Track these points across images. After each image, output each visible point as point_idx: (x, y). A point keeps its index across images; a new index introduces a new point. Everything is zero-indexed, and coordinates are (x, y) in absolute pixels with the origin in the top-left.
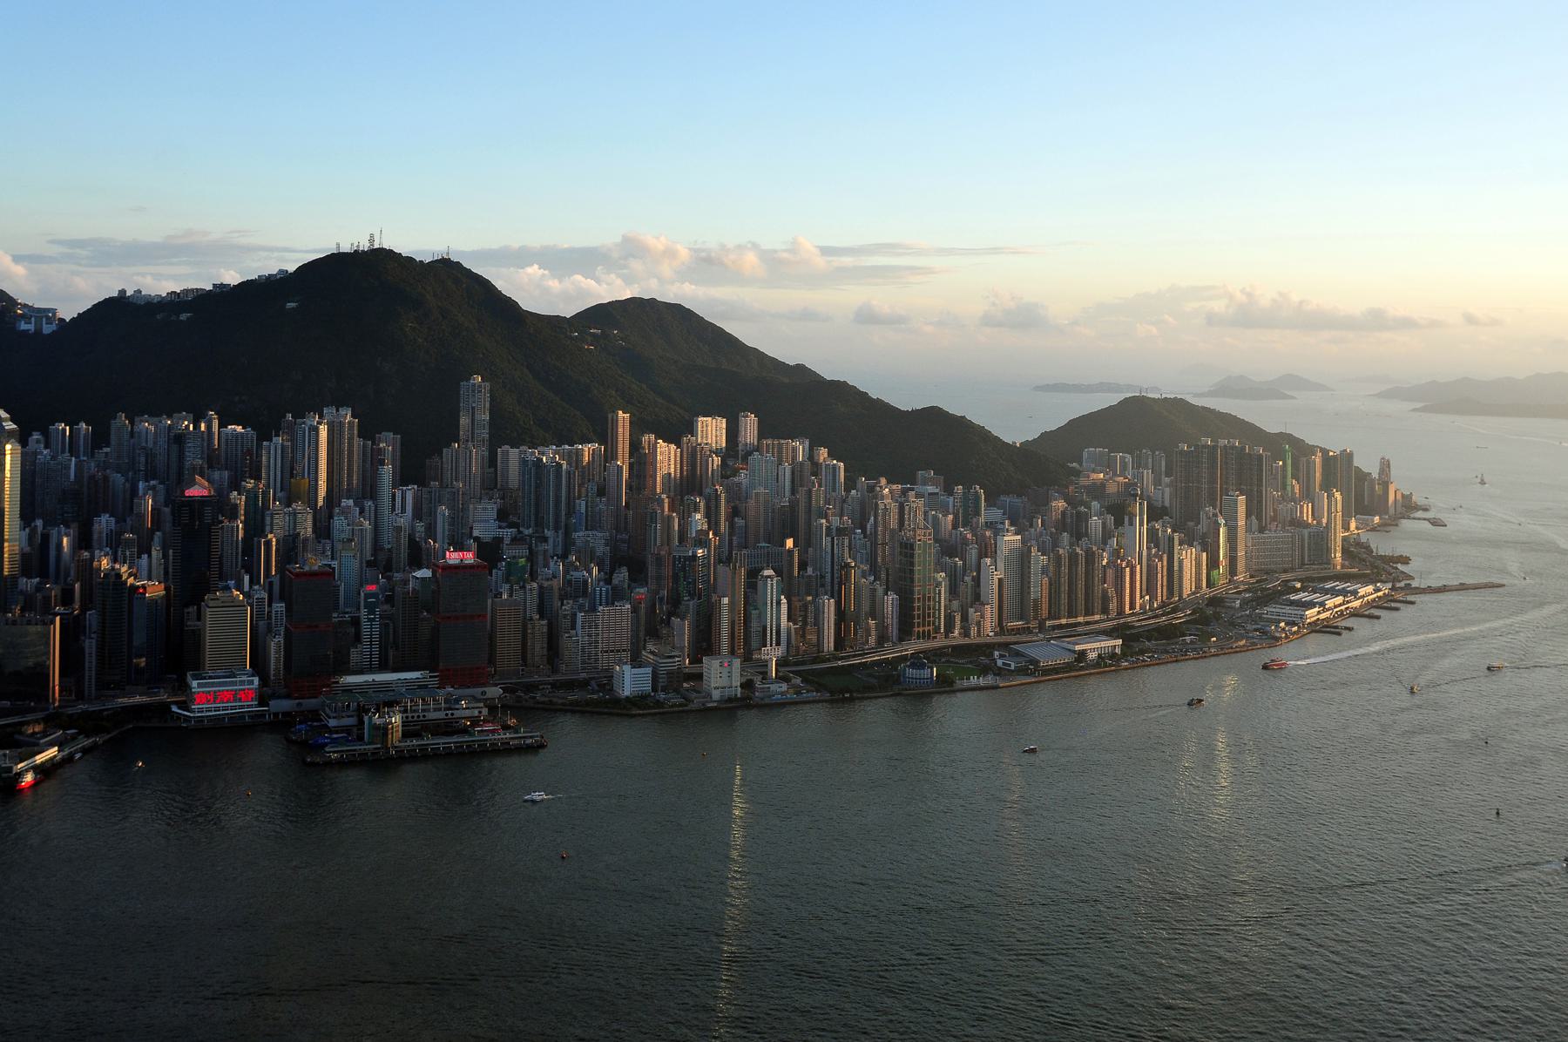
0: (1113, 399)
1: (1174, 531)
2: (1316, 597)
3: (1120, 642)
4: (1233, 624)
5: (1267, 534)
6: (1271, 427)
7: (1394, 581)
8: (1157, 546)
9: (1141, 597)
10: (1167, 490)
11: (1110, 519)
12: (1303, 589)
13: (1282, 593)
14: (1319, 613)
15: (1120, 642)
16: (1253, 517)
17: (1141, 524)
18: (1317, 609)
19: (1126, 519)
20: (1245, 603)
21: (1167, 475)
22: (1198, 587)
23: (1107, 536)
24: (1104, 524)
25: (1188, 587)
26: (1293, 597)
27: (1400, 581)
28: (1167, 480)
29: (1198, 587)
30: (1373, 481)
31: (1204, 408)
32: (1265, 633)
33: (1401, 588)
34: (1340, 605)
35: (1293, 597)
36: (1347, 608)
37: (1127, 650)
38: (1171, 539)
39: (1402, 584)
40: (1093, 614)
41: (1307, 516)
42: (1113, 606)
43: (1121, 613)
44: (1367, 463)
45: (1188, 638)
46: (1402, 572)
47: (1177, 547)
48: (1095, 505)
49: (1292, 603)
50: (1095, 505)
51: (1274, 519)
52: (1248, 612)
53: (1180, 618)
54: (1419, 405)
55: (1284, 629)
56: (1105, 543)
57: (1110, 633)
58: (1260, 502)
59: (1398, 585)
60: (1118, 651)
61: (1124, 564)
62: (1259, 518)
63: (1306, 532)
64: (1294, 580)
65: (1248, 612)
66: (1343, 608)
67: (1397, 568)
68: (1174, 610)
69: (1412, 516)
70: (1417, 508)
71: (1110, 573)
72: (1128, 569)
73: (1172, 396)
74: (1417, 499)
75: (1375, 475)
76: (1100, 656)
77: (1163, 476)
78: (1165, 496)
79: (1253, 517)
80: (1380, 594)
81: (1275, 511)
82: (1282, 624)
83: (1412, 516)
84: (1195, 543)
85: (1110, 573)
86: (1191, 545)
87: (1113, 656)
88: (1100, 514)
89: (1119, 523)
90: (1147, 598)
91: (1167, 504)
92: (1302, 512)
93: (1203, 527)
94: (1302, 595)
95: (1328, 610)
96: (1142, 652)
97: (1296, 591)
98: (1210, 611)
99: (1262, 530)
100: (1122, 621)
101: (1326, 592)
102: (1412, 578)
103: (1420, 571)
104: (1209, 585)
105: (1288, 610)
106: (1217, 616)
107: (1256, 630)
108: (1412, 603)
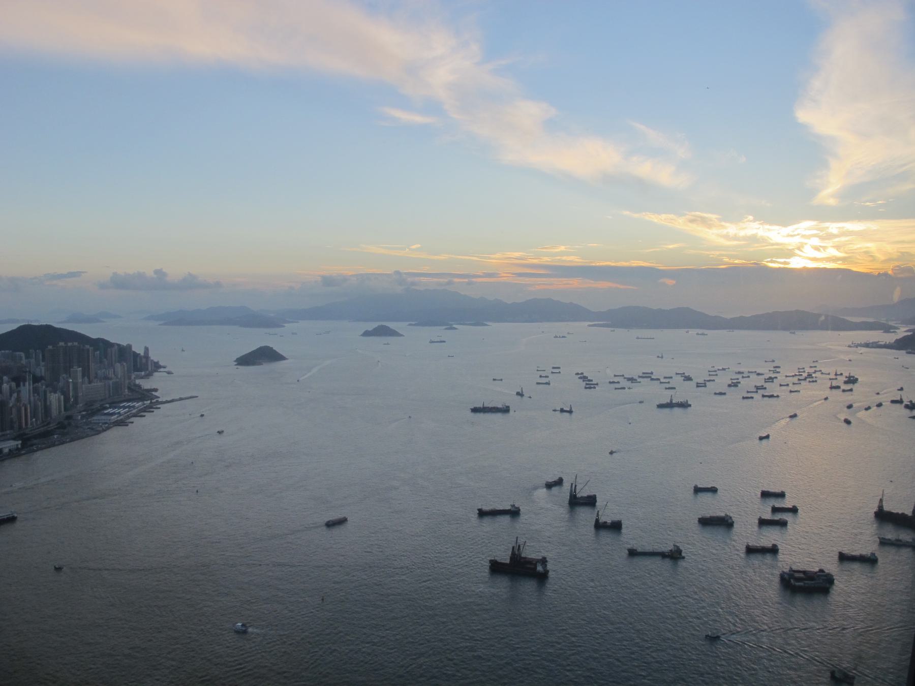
0: (14, 326)
1: (47, 387)
2: (116, 411)
3: (20, 442)
4: (77, 427)
5: (93, 384)
6: (94, 336)
7: (152, 399)
8: (38, 394)
9: (31, 420)
10: (43, 369)
11: (13, 384)
12: (110, 408)
13: (99, 410)
14: (118, 417)
15: (20, 442)
16: (86, 378)
17: (29, 385)
18: (116, 416)
19: (22, 384)
20: (83, 417)
21: (43, 361)
22: (60, 412)
23: (11, 392)
24: (10, 387)
25: (54, 412)
26: (106, 412)
27: (154, 399)
28: (43, 363)
29: (60, 412)
30: (141, 357)
31: (60, 329)
32: (92, 429)
33: (154, 402)
34: (127, 413)
35: (106, 412)
36: (130, 414)
37: (24, 445)
38: (45, 392)
39: (155, 400)
40: (6, 430)
41: (111, 375)
42: (16, 426)
43: (20, 427)
44: (139, 349)
45: (55, 436)
46: (155, 396)
47: (48, 395)
48: (5, 378)
49: (106, 414)
50: (5, 378)
51: (96, 377)
52: (84, 421)
53: (52, 426)
54: (162, 322)
55: (101, 426)
56: (11, 395)
57: (15, 439)
58: (89, 369)
59: (153, 401)
60: (19, 446)
61: (21, 405)
62: (89, 378)
63: (111, 382)
64: (106, 404)
65: (84, 421)
66: (128, 414)
67: (152, 394)
68: (49, 424)
69: (159, 370)
70: (160, 367)
71: (14, 410)
72: (23, 408)
73: (45, 324)
74: (161, 363)
75: (142, 354)
76: (10, 450)
77: (41, 362)
78: (41, 370)
79: (86, 378)
80: (145, 406)
81: (96, 374)
82: (100, 424)
83: (159, 370)
84: (58, 392)
85: (14, 410)
86: (55, 392)
87: (17, 449)
88: (8, 382)
89: (18, 385)
90: (34, 420)
91: (43, 375)
92: (109, 374)
93: (61, 384)
94: (110, 410)
95: (123, 415)
96: (32, 445)
97: (106, 408)
98: (66, 422)
99: (90, 382)
100: (22, 432)
101: (121, 407)
102: (159, 397)
103: (161, 395)
104: (66, 409)
105: (103, 417)
106: (69, 424)
107: (89, 428)
108: (159, 408)
